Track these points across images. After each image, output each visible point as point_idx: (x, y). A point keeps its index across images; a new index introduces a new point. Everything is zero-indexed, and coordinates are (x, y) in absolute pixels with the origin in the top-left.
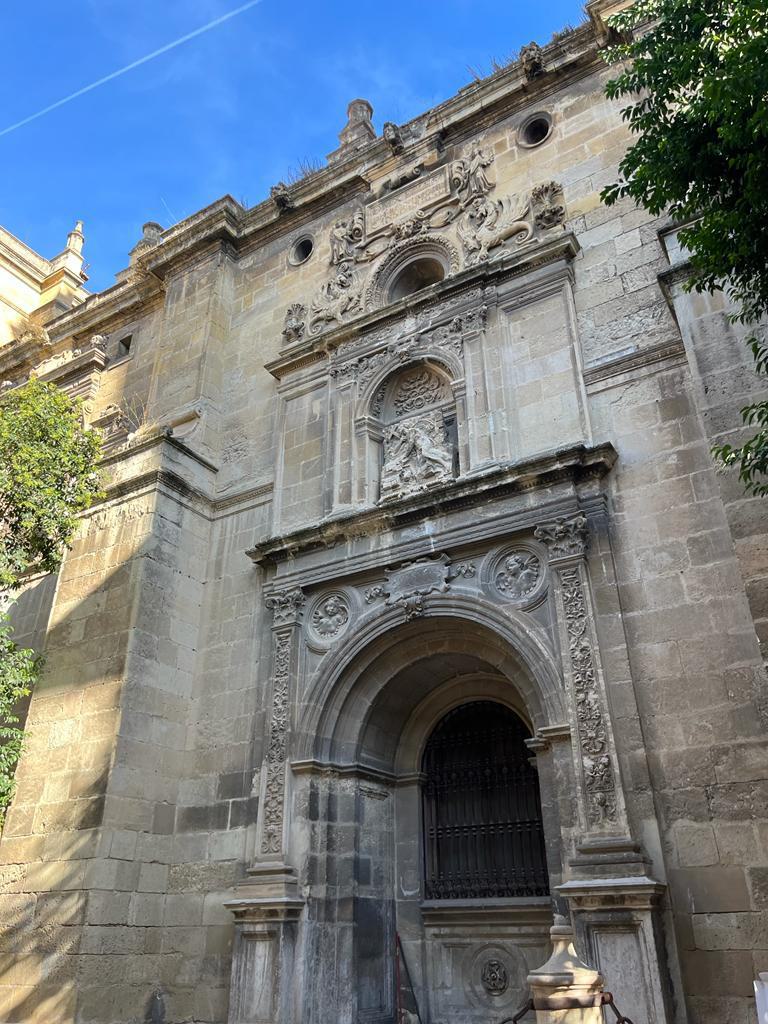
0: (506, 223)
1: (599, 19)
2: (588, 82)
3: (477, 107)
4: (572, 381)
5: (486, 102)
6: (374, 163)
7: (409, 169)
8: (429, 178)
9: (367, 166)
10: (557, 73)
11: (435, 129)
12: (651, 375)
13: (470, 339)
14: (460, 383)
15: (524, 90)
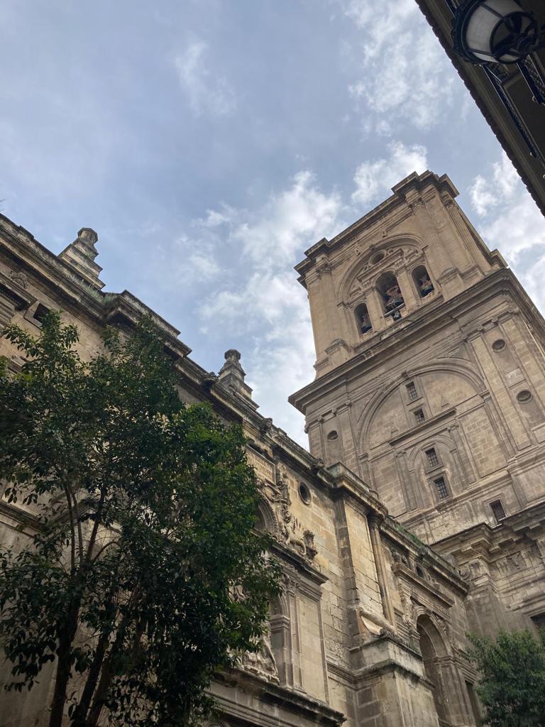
0: (298, 535)
1: (341, 481)
2: (320, 493)
3: (293, 455)
4: (321, 662)
5: (297, 458)
6: (251, 423)
7: (263, 447)
8: (266, 461)
9: (248, 420)
10: (317, 477)
11: (277, 442)
12: (344, 685)
13: (291, 595)
14: (288, 620)
15: (306, 469)
